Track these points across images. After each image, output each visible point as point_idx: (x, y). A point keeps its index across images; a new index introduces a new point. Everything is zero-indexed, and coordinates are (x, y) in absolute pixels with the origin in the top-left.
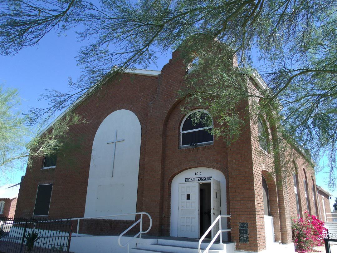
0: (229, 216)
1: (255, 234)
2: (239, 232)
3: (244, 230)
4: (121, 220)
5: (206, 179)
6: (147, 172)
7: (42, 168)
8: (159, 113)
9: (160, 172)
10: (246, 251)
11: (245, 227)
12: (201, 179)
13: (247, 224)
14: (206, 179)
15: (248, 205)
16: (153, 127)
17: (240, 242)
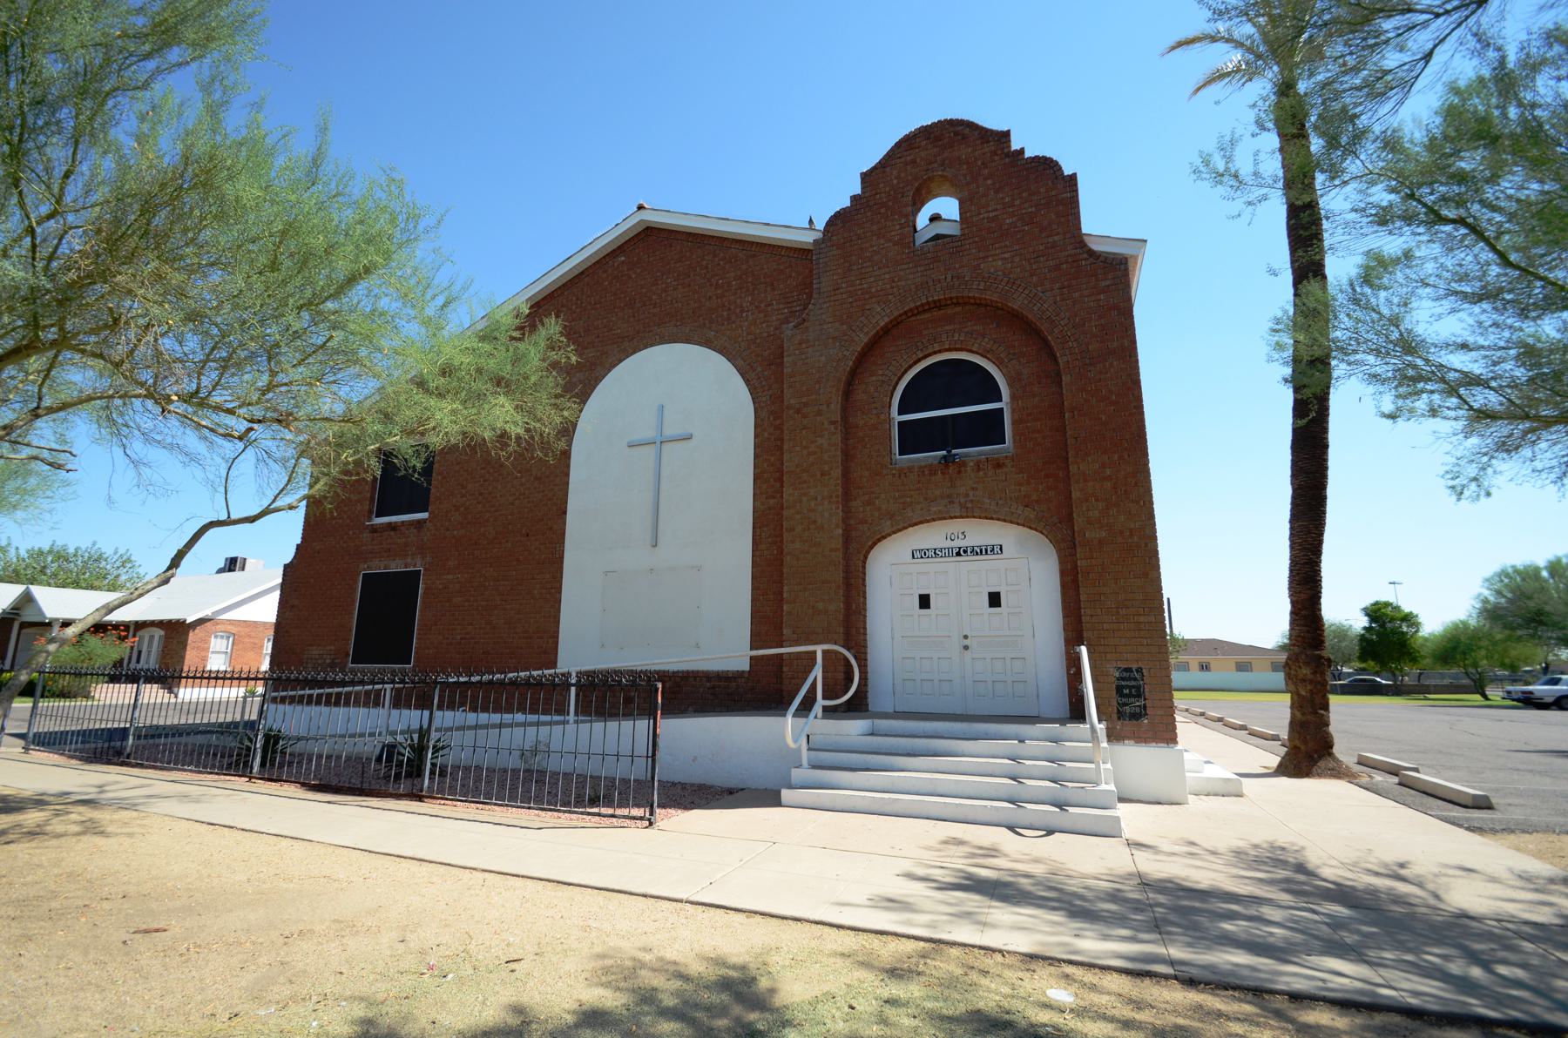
2: (1115, 692)
3: (1130, 687)
4: (698, 671)
5: (981, 550)
6: (792, 530)
7: (370, 519)
8: (823, 359)
9: (840, 531)
10: (1141, 742)
11: (1135, 679)
12: (965, 552)
13: (1139, 670)
14: (981, 550)
15: (1142, 619)
16: (804, 400)
17: (1119, 718)
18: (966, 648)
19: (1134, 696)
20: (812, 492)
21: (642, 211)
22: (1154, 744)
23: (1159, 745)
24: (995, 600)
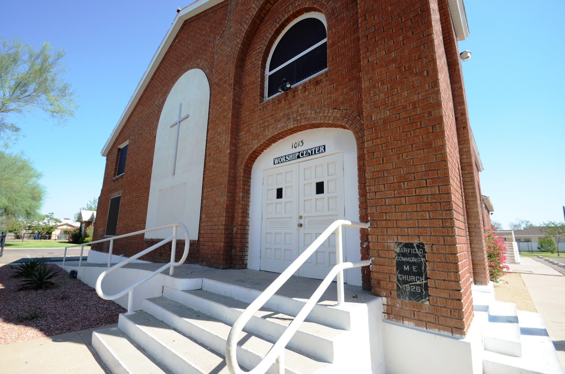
0: (367, 226)
1: (453, 279)
2: (395, 268)
3: (411, 264)
5: (312, 152)
9: (228, 151)
10: (422, 326)
11: (416, 256)
12: (302, 154)
13: (421, 246)
14: (312, 152)
17: (398, 296)
18: (301, 225)
19: (415, 274)
20: (219, 130)
21: (180, 12)
22: (436, 331)
23: (442, 332)
24: (320, 188)
